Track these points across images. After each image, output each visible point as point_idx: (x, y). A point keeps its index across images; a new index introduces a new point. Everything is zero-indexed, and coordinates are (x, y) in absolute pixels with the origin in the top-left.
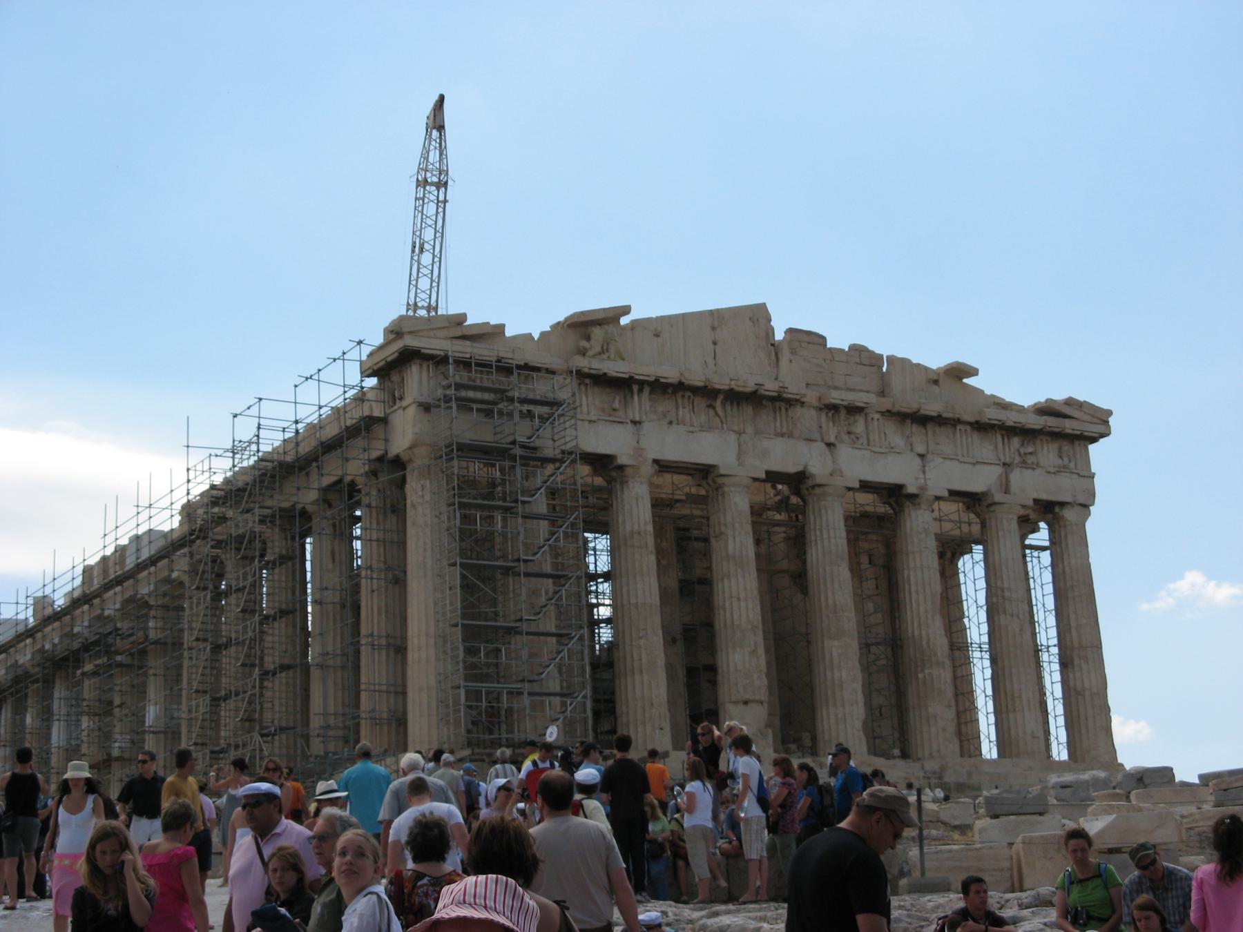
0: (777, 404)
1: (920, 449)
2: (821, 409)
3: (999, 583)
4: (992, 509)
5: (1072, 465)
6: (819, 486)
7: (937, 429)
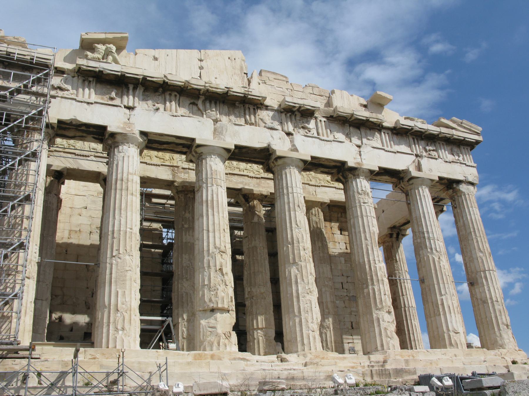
0: (247, 106)
1: (359, 142)
2: (281, 112)
3: (420, 229)
4: (411, 182)
5: (461, 158)
6: (280, 158)
7: (368, 132)
